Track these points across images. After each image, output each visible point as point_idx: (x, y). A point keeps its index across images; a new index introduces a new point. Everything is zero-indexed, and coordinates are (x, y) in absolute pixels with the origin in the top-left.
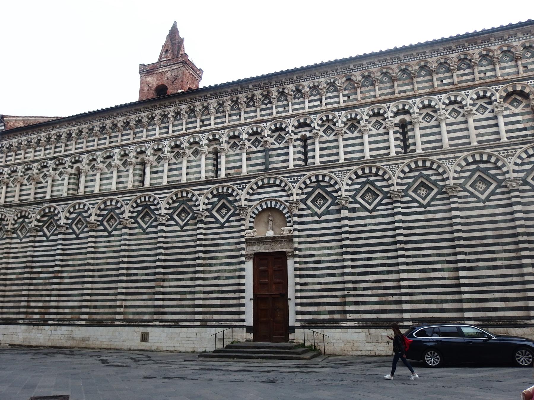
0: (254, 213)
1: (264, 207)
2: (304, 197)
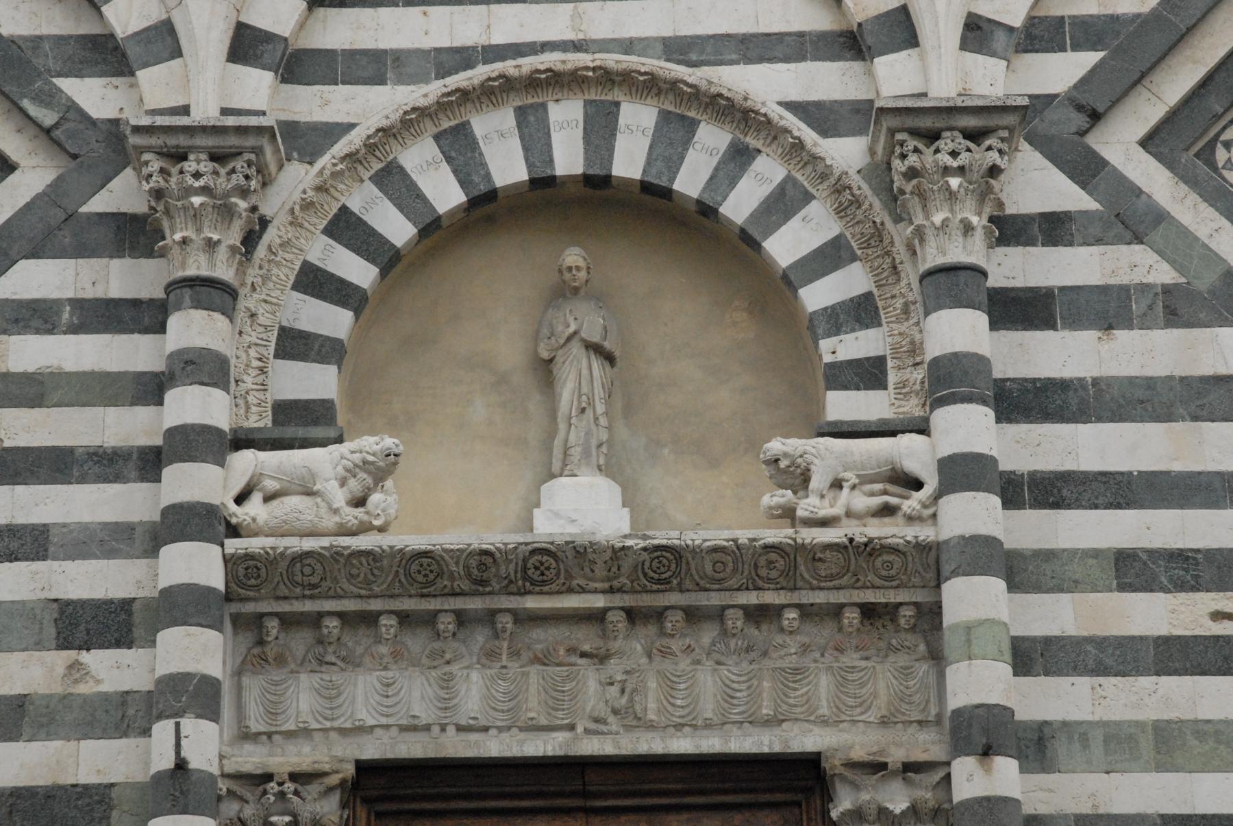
0: (348, 229)
1: (508, 167)
2: (1061, 71)
